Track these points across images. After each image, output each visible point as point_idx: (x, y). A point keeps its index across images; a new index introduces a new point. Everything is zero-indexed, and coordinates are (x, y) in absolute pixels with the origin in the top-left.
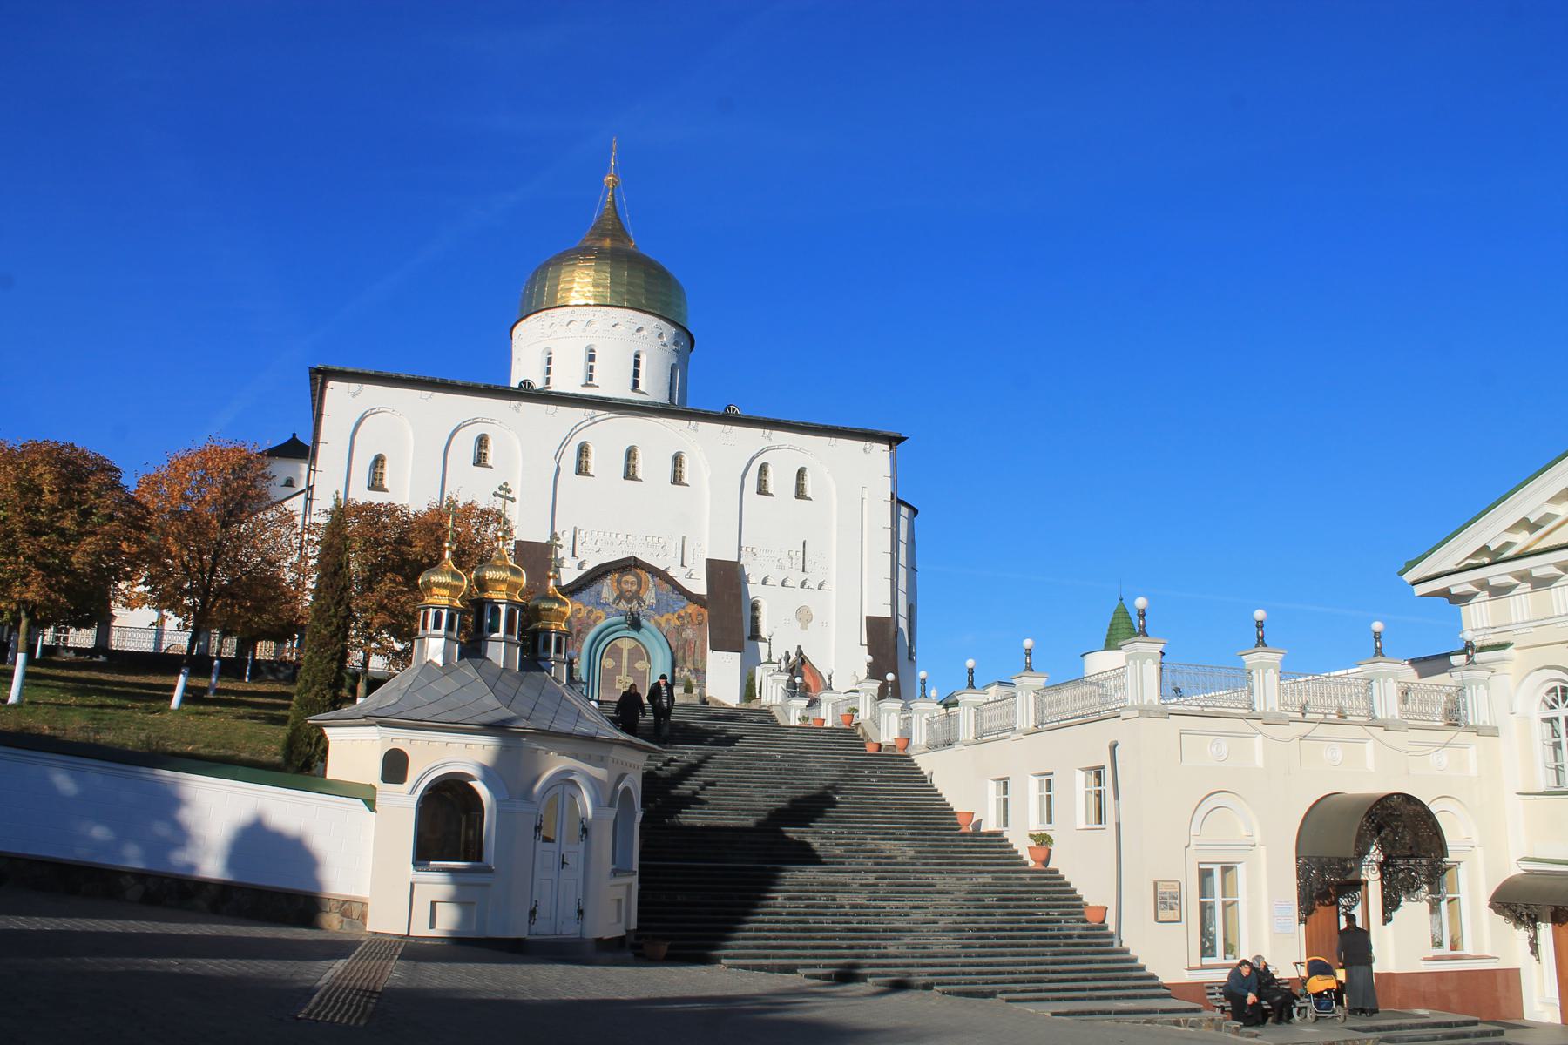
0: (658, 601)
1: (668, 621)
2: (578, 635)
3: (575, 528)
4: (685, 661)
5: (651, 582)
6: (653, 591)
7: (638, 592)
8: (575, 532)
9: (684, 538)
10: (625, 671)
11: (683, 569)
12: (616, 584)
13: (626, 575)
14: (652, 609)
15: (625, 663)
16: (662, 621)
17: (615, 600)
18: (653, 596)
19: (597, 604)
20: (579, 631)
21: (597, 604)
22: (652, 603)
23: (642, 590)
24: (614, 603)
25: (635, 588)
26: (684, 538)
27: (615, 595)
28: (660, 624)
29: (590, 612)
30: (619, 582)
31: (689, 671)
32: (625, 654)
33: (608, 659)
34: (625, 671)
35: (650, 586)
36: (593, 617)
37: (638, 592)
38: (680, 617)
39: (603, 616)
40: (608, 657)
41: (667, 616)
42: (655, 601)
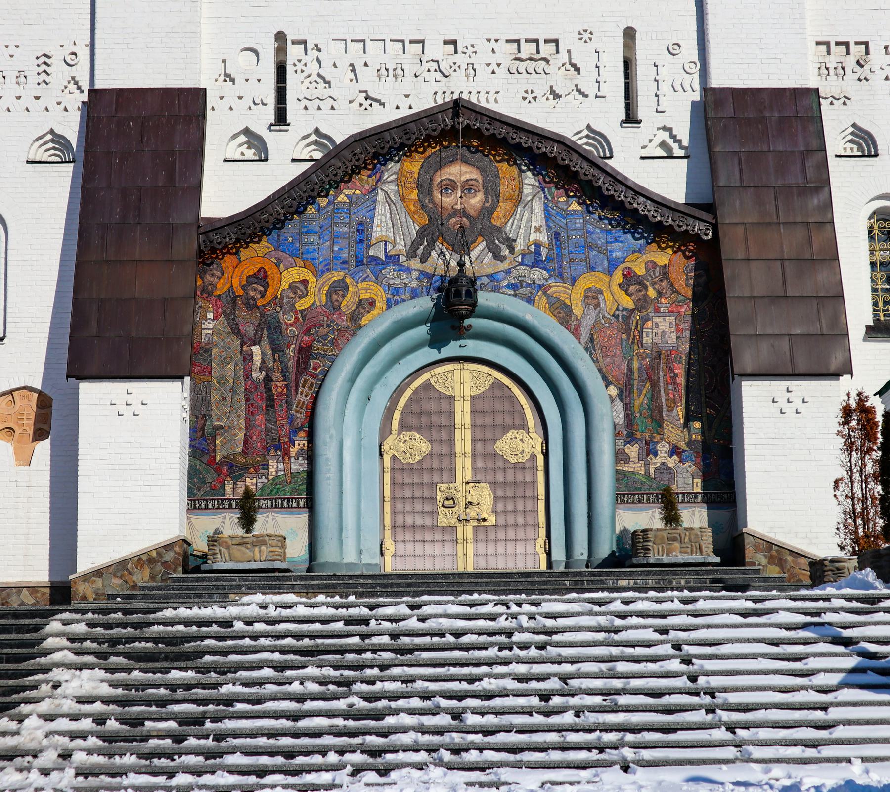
0: (557, 235)
1: (592, 298)
2: (302, 365)
3: (280, 37)
4: (659, 422)
5: (529, 179)
6: (538, 207)
7: (487, 212)
8: (281, 50)
9: (629, 34)
10: (464, 468)
11: (630, 131)
12: (414, 195)
13: (451, 161)
14: (537, 263)
15: (463, 441)
16: (576, 300)
17: (415, 245)
18: (538, 219)
19: (359, 262)
20: (305, 353)
21: (359, 262)
22: (538, 245)
23: (503, 207)
24: (412, 254)
25: (476, 201)
26: (629, 34)
27: (414, 229)
28: (569, 309)
29: (340, 288)
30: (424, 187)
31: (675, 451)
32: (463, 415)
33: (406, 436)
34: (464, 468)
35: (527, 190)
36: (348, 303)
37: (487, 212)
38: (629, 278)
39: (380, 295)
40: (404, 427)
41: (587, 282)
42: (543, 238)
